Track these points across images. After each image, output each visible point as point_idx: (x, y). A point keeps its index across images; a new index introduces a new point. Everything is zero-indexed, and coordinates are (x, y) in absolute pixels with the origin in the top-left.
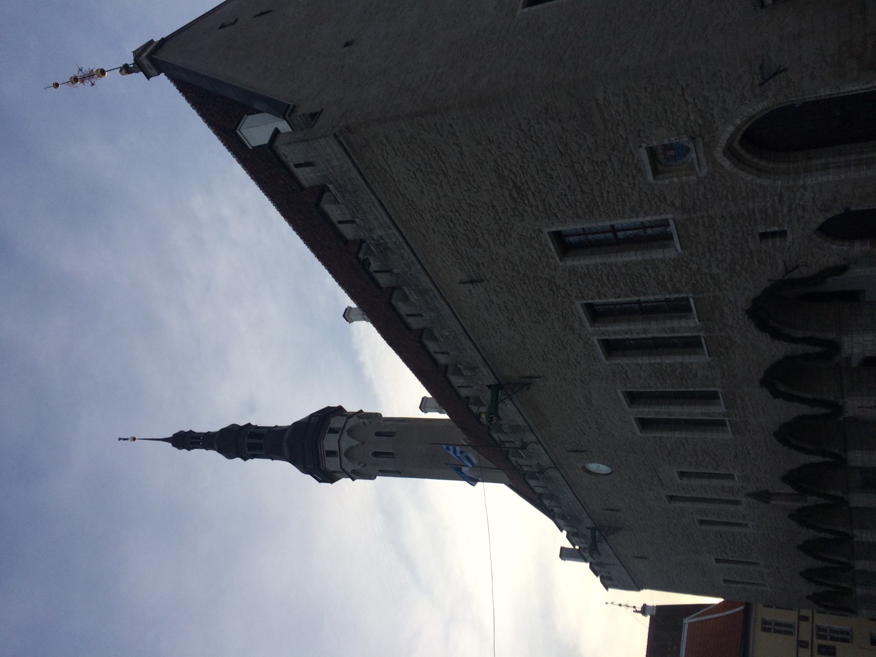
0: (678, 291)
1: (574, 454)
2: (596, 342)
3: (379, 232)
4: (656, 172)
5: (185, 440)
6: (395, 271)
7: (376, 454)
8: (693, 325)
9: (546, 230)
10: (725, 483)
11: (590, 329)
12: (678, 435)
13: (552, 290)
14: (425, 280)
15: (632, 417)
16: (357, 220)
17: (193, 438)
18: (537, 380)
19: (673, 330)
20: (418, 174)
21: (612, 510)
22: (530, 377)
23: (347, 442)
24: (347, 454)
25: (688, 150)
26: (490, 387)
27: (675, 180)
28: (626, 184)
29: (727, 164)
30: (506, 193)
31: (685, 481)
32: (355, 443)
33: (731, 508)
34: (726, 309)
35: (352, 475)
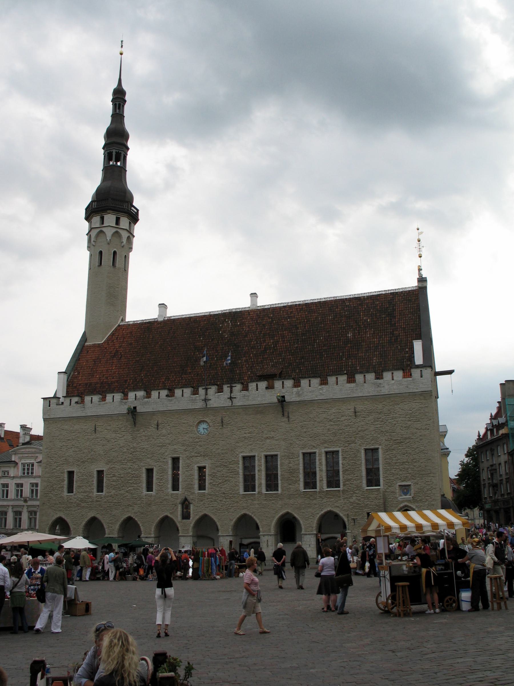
0: (344, 485)
1: (219, 419)
2: (315, 451)
3: (387, 387)
4: (400, 486)
5: (119, 97)
6: (365, 384)
7: (115, 253)
8: (324, 487)
9: (380, 447)
10: (196, 486)
11: (323, 450)
12: (241, 471)
13: (348, 441)
14: (360, 395)
15: (256, 455)
16: (393, 382)
17: (119, 105)
18: (287, 420)
19: (321, 481)
20: (411, 412)
21: (158, 426)
22: (288, 417)
23: (125, 235)
24: (117, 232)
25: (406, 495)
26: (283, 397)
27: (397, 491)
28: (398, 476)
29: (402, 505)
30: (399, 439)
31: (196, 468)
32: (125, 240)
33: (170, 485)
34: (333, 499)
35: (98, 230)
